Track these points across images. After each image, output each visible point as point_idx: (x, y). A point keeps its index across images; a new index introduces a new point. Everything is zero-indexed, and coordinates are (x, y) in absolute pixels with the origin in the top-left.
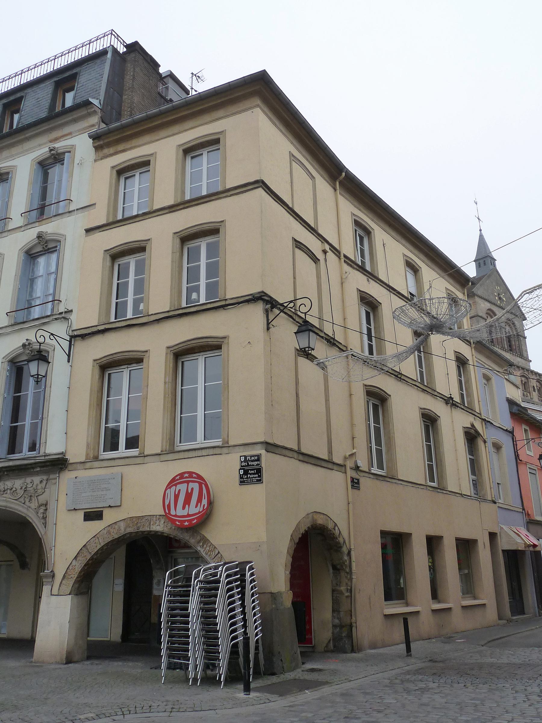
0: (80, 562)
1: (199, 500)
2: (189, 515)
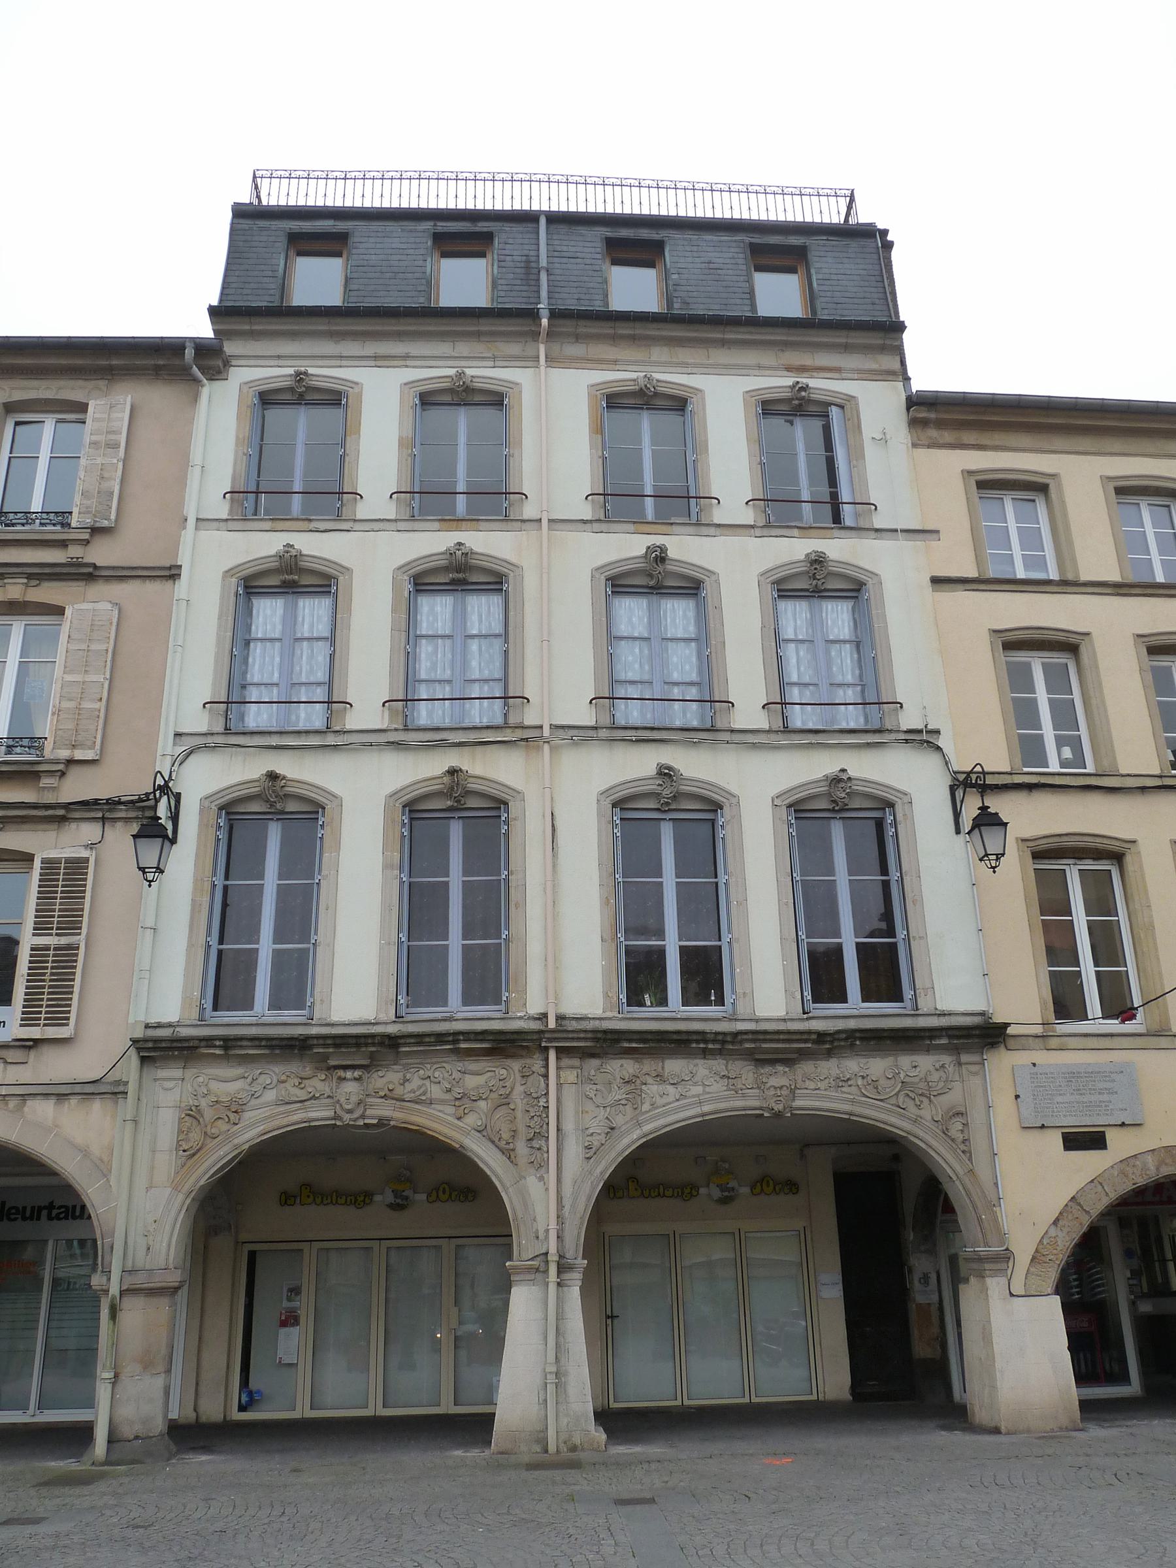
0: (1066, 1230)
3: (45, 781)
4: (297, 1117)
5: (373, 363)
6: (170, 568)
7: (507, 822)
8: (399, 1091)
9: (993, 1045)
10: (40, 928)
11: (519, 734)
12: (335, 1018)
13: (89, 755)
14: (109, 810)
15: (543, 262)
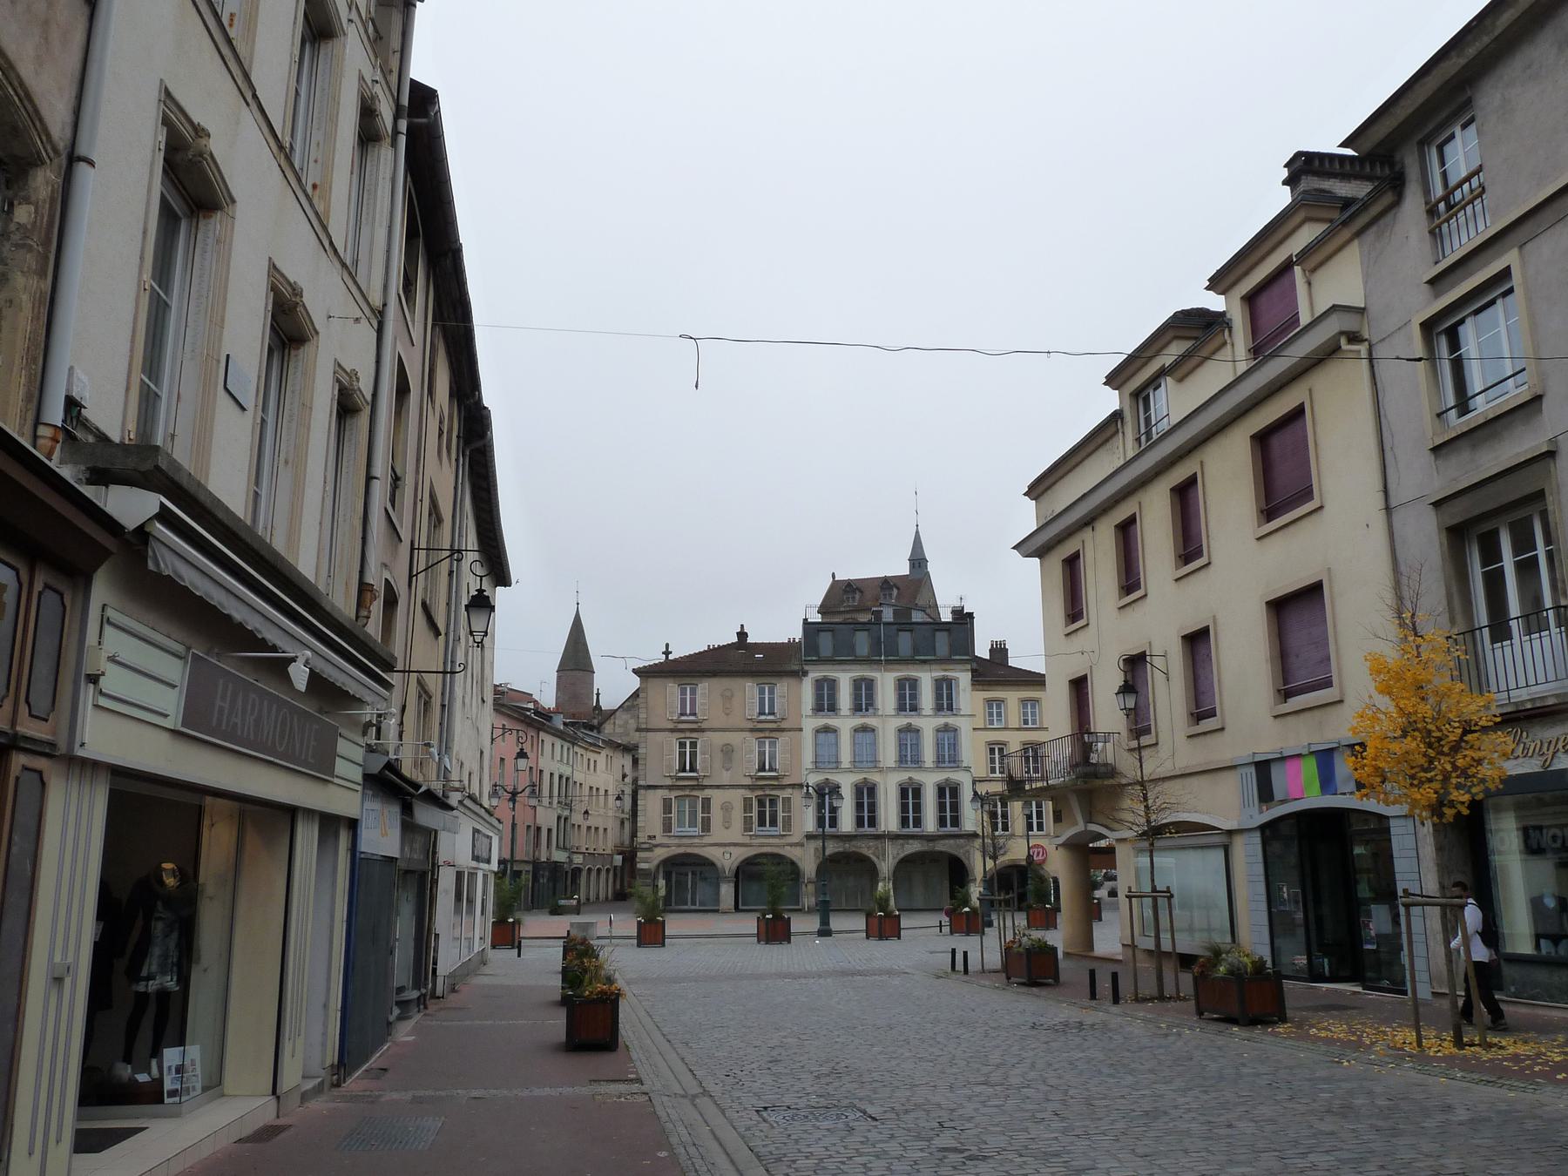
4: (837, 850)
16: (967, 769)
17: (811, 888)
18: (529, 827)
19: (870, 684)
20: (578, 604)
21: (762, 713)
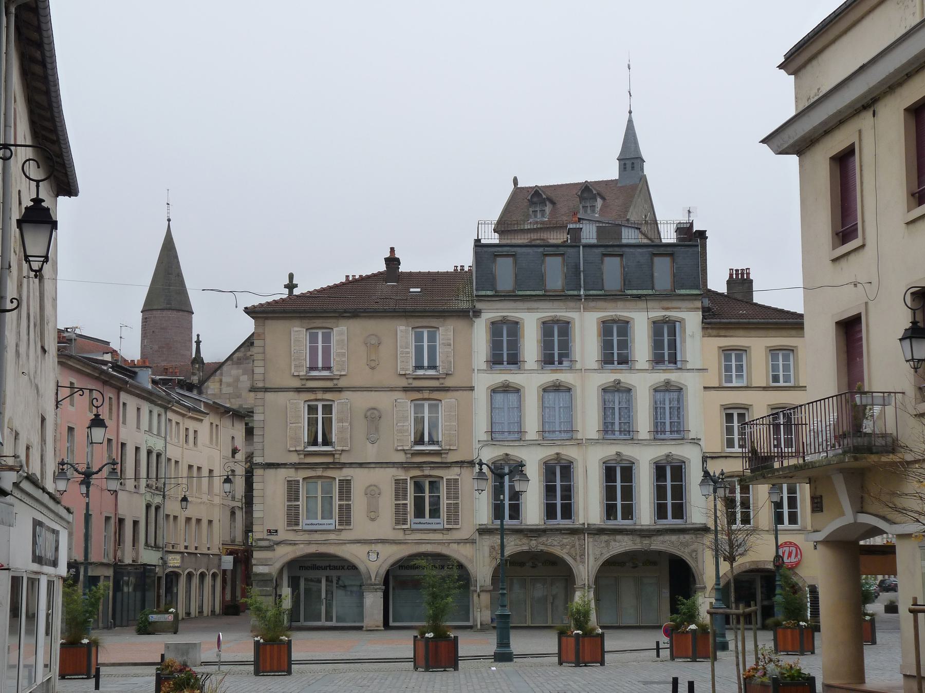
1: (796, 555)
2: (791, 562)
3: (443, 456)
4: (519, 549)
5: (526, 311)
6: (471, 387)
7: (573, 468)
8: (546, 543)
9: (707, 533)
10: (448, 498)
11: (576, 441)
12: (528, 524)
13: (455, 448)
14: (463, 464)
15: (582, 269)
16: (695, 442)
17: (485, 598)
18: (108, 519)
19: (565, 327)
20: (169, 220)
21: (419, 367)
